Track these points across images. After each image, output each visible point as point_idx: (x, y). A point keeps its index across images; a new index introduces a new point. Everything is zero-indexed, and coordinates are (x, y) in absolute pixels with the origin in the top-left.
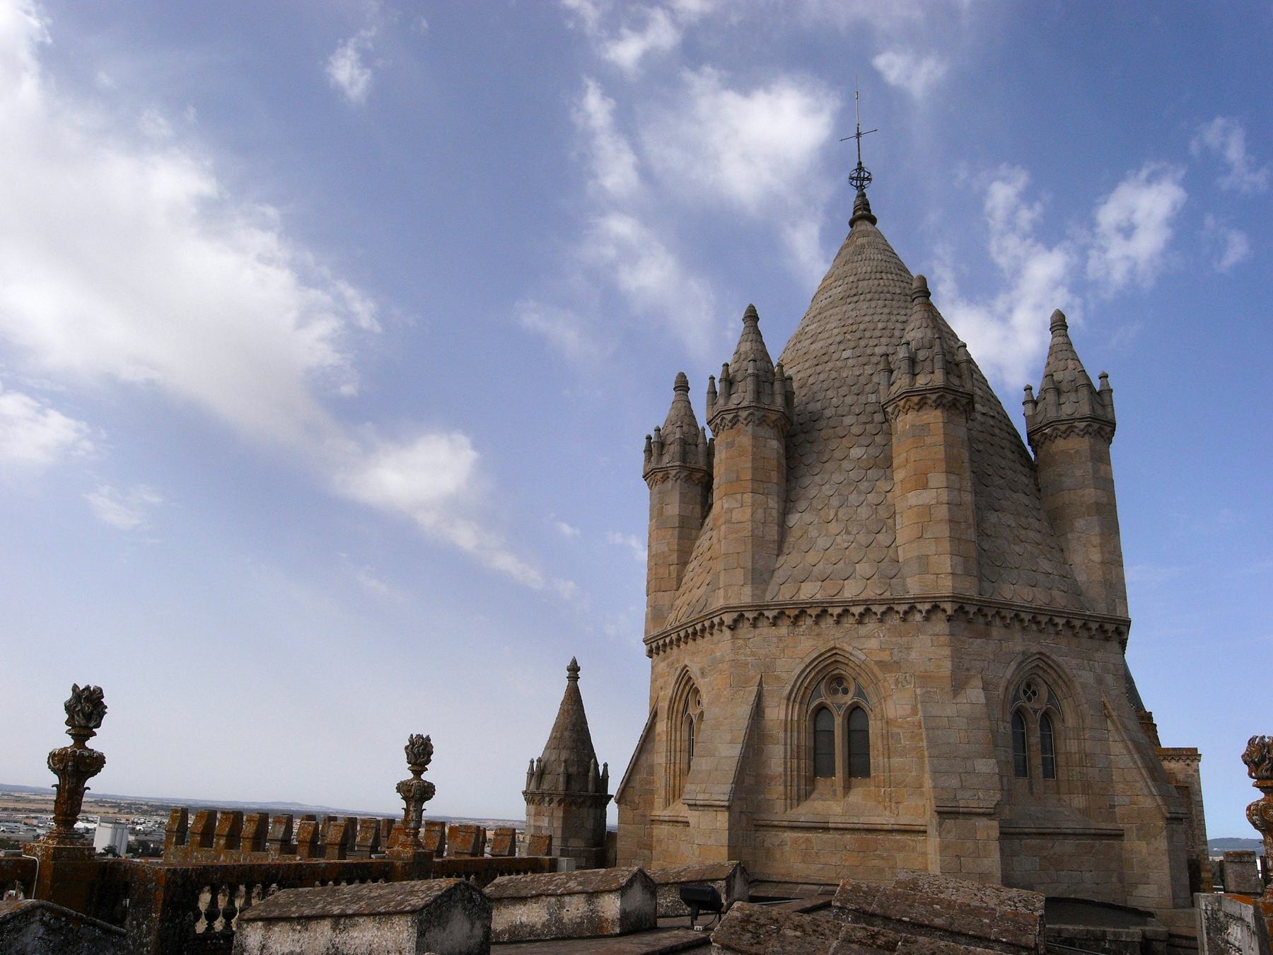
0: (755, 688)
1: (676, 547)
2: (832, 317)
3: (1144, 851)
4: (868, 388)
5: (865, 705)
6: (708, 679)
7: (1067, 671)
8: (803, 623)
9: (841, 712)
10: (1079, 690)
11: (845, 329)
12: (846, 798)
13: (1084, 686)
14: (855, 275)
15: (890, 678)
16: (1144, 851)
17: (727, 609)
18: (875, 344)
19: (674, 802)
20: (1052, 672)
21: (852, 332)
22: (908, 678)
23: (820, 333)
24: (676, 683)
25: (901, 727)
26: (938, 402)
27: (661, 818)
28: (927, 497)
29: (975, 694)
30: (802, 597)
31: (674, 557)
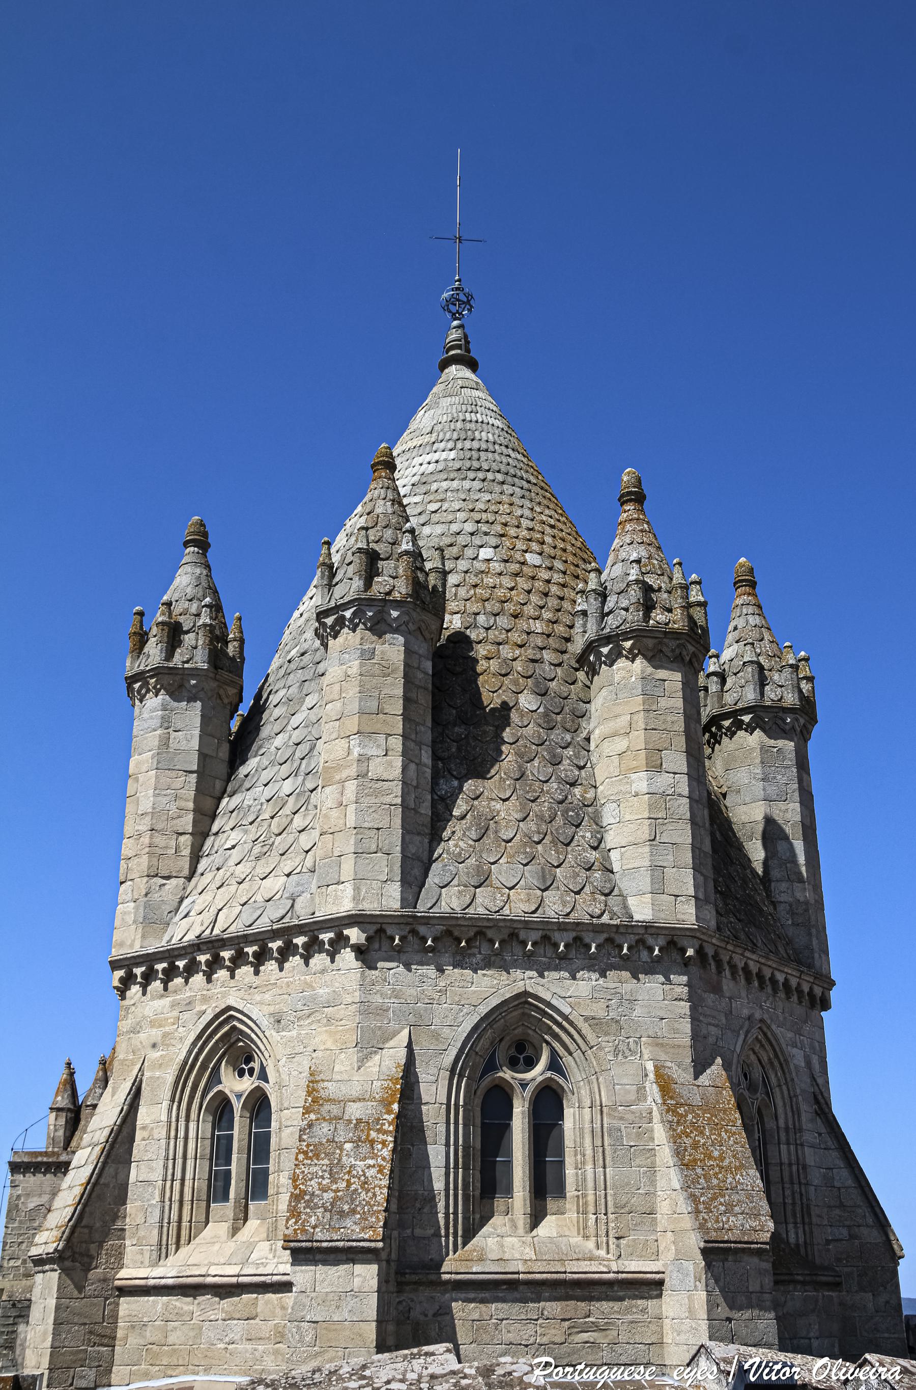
0: (401, 1055)
1: (191, 805)
2: (449, 494)
3: (870, 1305)
4: (529, 610)
5: (563, 1084)
6: (294, 1033)
7: (784, 1046)
8: (476, 951)
9: (528, 1093)
10: (794, 1074)
11: (477, 516)
12: (534, 1233)
13: (796, 1067)
14: (473, 440)
15: (607, 1044)
16: (870, 1305)
17: (355, 920)
18: (524, 548)
19: (177, 1249)
20: (768, 1047)
21: (487, 522)
22: (632, 1046)
23: (435, 512)
24: (199, 1037)
25: (621, 1118)
26: (677, 651)
27: (151, 1282)
28: (664, 781)
29: (716, 1069)
30: (481, 910)
31: (187, 822)
